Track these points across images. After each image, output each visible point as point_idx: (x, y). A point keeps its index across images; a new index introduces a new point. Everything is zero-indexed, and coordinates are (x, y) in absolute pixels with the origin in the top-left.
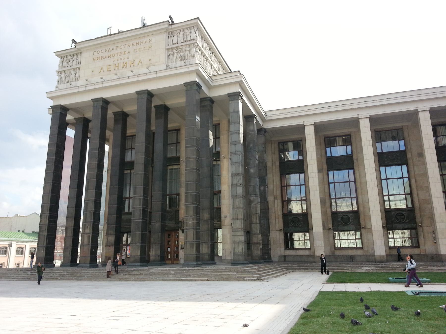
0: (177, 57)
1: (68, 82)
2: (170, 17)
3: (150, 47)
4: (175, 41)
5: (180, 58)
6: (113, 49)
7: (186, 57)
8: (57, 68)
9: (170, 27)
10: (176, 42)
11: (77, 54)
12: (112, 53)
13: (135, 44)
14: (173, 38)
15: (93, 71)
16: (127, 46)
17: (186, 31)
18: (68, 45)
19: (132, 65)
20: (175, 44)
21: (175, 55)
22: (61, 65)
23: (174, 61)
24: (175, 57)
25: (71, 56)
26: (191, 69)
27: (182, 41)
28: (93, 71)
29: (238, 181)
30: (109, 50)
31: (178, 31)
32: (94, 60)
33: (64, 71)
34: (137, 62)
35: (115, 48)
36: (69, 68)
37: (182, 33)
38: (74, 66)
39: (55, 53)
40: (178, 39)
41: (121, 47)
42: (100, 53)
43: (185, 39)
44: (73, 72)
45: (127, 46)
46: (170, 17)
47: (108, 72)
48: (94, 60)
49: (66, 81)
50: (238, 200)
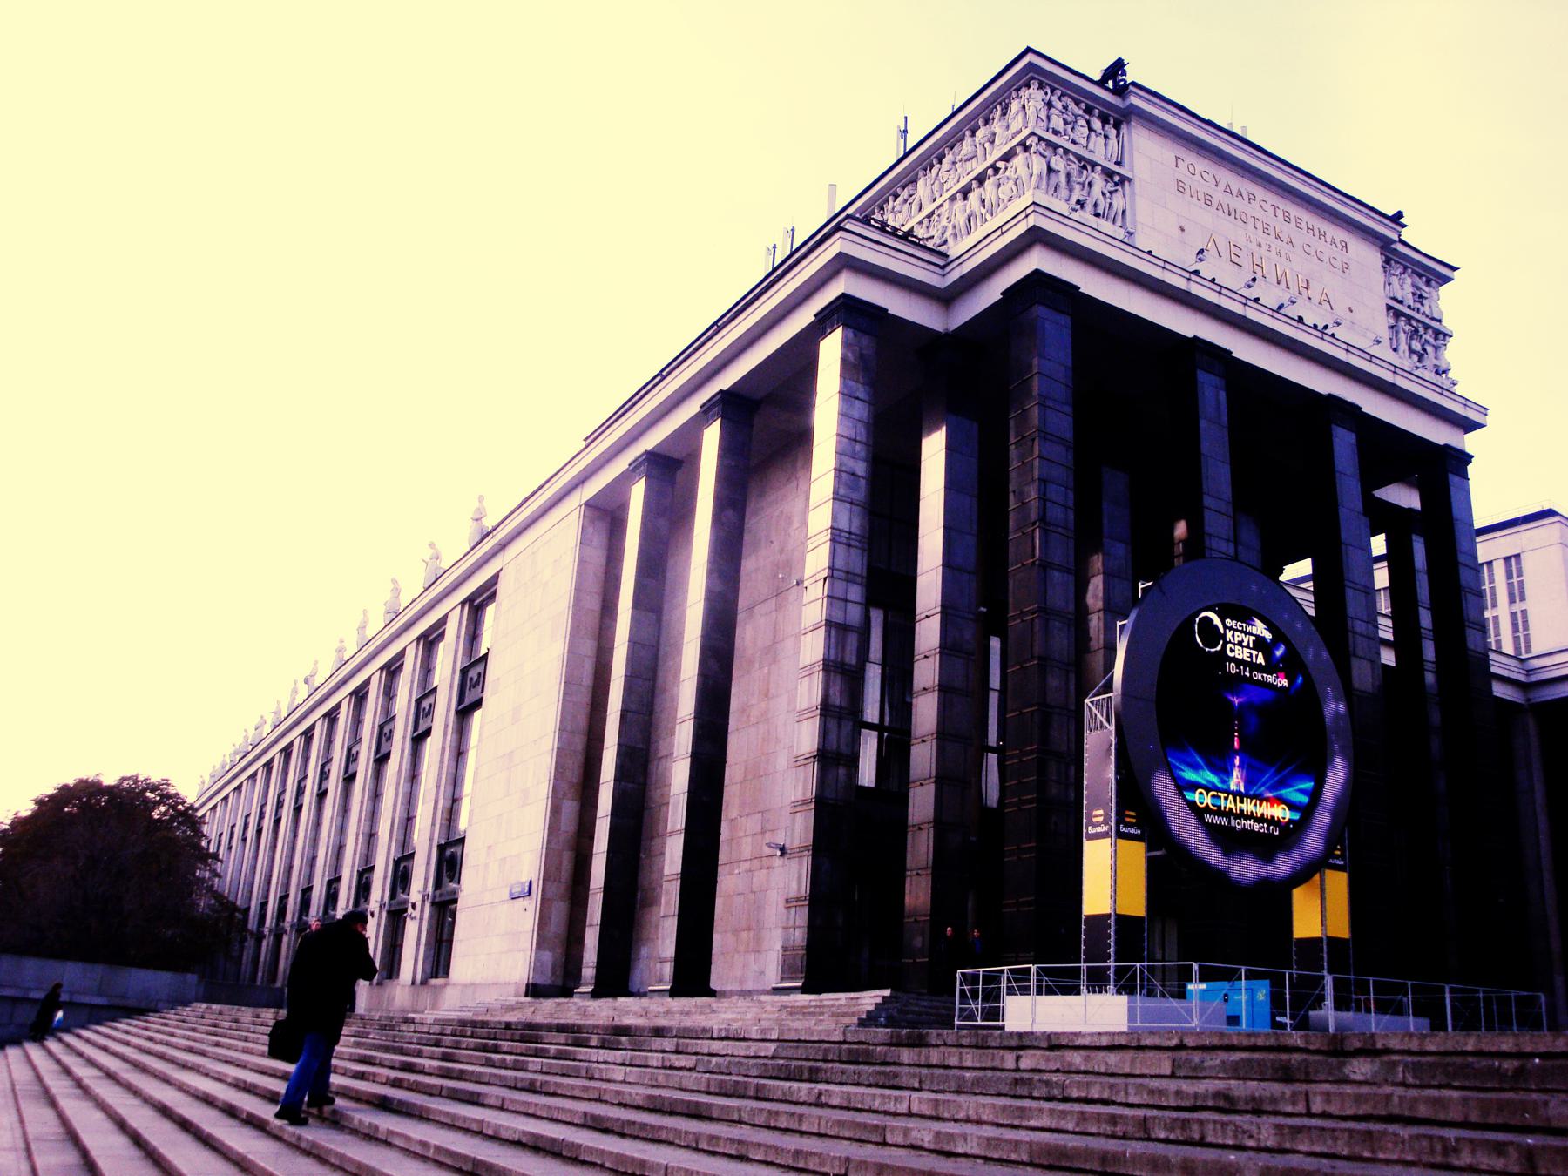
3: (1346, 267)
12: (1238, 204)
16: (1280, 213)
25: (1077, 103)
30: (1228, 190)
33: (1066, 151)
34: (1315, 293)
38: (1098, 157)
40: (1404, 288)
42: (1198, 176)
45: (1280, 213)
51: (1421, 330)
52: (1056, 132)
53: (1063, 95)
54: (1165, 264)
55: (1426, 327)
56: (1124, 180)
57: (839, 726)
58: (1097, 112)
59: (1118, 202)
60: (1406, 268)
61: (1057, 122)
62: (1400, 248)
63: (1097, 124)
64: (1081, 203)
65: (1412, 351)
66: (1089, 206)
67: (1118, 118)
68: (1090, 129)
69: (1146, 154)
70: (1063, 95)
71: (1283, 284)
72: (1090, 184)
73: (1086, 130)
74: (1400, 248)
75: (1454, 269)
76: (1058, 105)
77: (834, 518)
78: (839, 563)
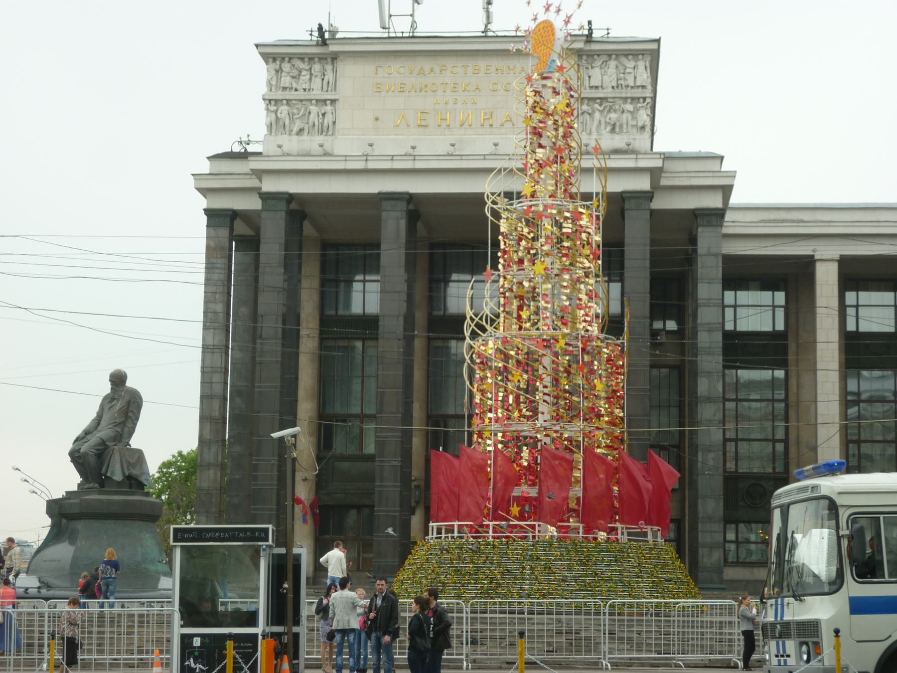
0: (600, 121)
1: (300, 131)
2: (590, 23)
4: (595, 82)
5: (609, 128)
6: (432, 70)
7: (625, 126)
8: (264, 89)
9: (588, 47)
10: (598, 83)
11: (320, 59)
13: (493, 69)
14: (591, 72)
15: (377, 119)
16: (470, 70)
17: (624, 60)
18: (300, 31)
19: (487, 123)
20: (597, 87)
21: (597, 115)
22: (274, 83)
23: (594, 129)
24: (596, 123)
25: (302, 59)
26: (643, 164)
27: (614, 84)
28: (377, 119)
29: (715, 415)
30: (421, 72)
31: (605, 58)
32: (378, 88)
35: (437, 69)
36: (301, 95)
37: (613, 64)
38: (317, 93)
39: (257, 46)
41: (455, 70)
43: (620, 82)
44: (313, 109)
45: (470, 70)
46: (590, 23)
47: (422, 130)
48: (378, 88)
49: (295, 129)
50: (712, 455)
51: (619, 102)
52: (285, 88)
53: (290, 59)
54: (346, 158)
55: (625, 99)
56: (333, 101)
57: (209, 449)
58: (316, 59)
59: (329, 119)
60: (610, 56)
61: (286, 81)
62: (594, 47)
63: (317, 67)
64: (300, 131)
65: (607, 123)
66: (306, 132)
67: (334, 57)
68: (311, 74)
69: (351, 77)
70: (290, 59)
71: (466, 125)
72: (310, 113)
73: (308, 77)
74: (594, 47)
75: (658, 41)
76: (286, 66)
77: (204, 339)
78: (207, 364)
